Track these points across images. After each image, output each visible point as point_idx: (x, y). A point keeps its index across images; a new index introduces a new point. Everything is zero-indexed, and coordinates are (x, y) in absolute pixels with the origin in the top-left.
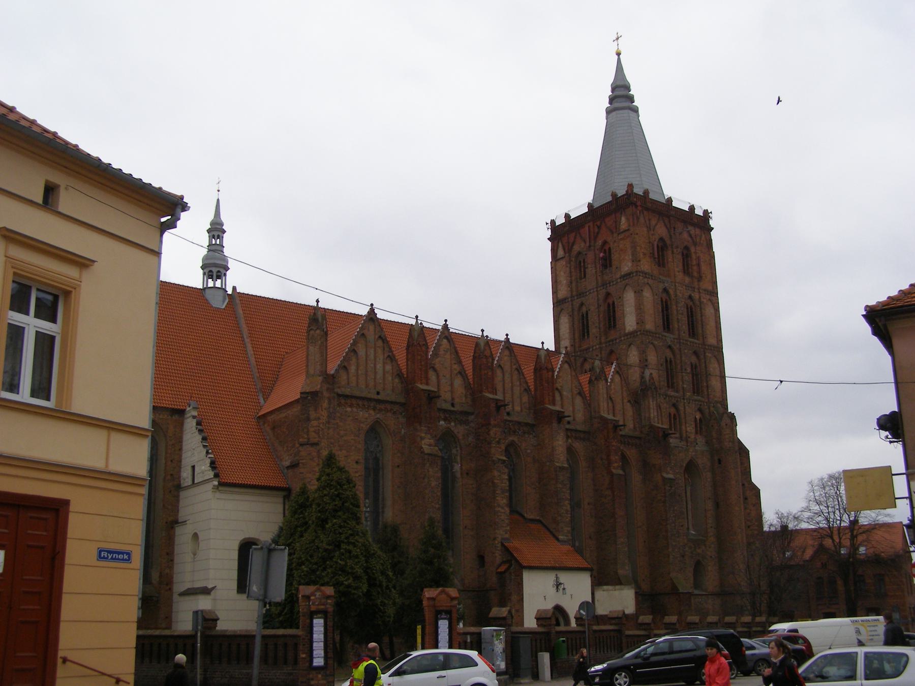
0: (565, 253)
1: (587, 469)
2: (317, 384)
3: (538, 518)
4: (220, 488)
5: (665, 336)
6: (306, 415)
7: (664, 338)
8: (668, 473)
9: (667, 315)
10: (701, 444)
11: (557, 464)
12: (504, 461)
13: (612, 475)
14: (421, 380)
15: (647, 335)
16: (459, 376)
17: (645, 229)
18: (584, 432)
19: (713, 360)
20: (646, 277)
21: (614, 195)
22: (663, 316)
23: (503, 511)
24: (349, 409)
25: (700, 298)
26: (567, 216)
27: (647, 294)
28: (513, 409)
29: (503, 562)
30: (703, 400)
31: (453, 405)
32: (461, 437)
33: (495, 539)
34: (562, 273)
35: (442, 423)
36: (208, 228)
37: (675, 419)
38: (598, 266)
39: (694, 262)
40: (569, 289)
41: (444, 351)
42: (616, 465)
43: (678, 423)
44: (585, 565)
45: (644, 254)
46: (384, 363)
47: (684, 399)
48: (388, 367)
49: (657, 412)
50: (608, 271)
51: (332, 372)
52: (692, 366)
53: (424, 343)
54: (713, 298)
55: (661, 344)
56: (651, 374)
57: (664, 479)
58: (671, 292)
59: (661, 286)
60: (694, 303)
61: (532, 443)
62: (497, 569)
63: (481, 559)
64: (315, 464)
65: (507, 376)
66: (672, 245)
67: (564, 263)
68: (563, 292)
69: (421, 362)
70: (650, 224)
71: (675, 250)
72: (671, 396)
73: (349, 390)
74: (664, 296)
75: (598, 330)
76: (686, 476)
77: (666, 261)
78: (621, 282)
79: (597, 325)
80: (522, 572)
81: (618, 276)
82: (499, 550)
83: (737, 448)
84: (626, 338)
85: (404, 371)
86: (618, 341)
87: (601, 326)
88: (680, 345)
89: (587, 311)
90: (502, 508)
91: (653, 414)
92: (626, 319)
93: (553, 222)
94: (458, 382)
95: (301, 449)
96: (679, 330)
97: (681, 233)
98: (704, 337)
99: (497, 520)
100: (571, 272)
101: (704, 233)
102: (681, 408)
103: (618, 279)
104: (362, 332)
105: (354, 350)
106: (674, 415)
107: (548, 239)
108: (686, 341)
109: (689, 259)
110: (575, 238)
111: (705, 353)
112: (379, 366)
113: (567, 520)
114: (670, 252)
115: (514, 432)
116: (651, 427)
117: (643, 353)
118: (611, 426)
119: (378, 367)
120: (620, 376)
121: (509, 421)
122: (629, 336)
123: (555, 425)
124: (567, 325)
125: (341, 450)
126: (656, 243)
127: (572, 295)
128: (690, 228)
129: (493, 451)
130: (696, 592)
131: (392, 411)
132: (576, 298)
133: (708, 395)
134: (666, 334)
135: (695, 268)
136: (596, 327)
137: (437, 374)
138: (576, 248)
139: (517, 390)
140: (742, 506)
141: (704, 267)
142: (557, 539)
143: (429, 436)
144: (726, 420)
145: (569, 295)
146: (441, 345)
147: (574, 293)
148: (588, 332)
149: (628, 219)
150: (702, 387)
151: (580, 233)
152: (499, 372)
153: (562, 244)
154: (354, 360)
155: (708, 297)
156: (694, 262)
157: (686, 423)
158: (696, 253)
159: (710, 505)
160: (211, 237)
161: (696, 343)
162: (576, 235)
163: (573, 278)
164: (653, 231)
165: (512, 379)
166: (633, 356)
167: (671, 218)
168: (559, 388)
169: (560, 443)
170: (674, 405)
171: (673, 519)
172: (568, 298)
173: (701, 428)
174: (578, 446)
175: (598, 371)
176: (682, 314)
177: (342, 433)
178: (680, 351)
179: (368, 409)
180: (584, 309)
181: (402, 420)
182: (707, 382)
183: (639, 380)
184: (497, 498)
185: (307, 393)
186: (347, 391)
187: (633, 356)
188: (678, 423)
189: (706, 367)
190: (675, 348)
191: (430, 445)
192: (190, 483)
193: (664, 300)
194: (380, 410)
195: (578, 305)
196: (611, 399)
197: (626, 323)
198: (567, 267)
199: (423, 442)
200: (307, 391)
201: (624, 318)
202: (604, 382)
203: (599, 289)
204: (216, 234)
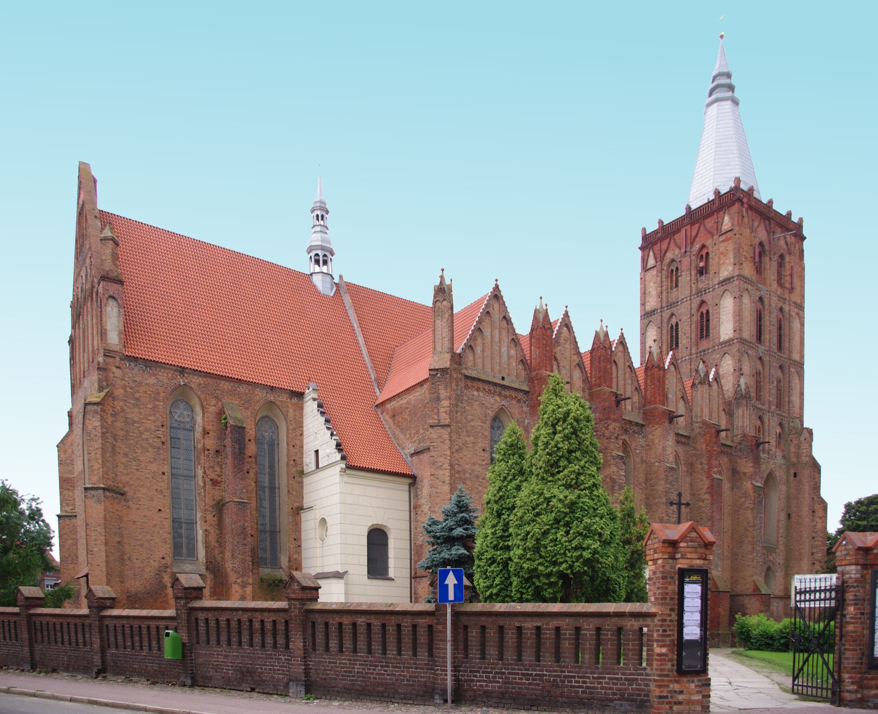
2: (445, 361)
9: (760, 326)
12: (622, 458)
18: (685, 437)
19: (796, 377)
24: (476, 393)
26: (661, 222)
38: (693, 273)
42: (716, 469)
46: (509, 347)
48: (513, 352)
50: (703, 277)
51: (458, 351)
55: (754, 354)
65: (620, 372)
92: (721, 327)
95: (431, 430)
98: (790, 352)
103: (714, 286)
106: (759, 427)
108: (775, 353)
110: (669, 244)
112: (504, 349)
125: (469, 436)
133: (789, 410)
134: (759, 346)
138: (669, 256)
144: (805, 434)
154: (480, 341)
157: (769, 436)
165: (625, 377)
174: (680, 449)
175: (702, 375)
177: (470, 417)
182: (789, 397)
185: (437, 370)
186: (474, 374)
194: (506, 397)
197: (721, 331)
200: (437, 368)
203: (692, 297)
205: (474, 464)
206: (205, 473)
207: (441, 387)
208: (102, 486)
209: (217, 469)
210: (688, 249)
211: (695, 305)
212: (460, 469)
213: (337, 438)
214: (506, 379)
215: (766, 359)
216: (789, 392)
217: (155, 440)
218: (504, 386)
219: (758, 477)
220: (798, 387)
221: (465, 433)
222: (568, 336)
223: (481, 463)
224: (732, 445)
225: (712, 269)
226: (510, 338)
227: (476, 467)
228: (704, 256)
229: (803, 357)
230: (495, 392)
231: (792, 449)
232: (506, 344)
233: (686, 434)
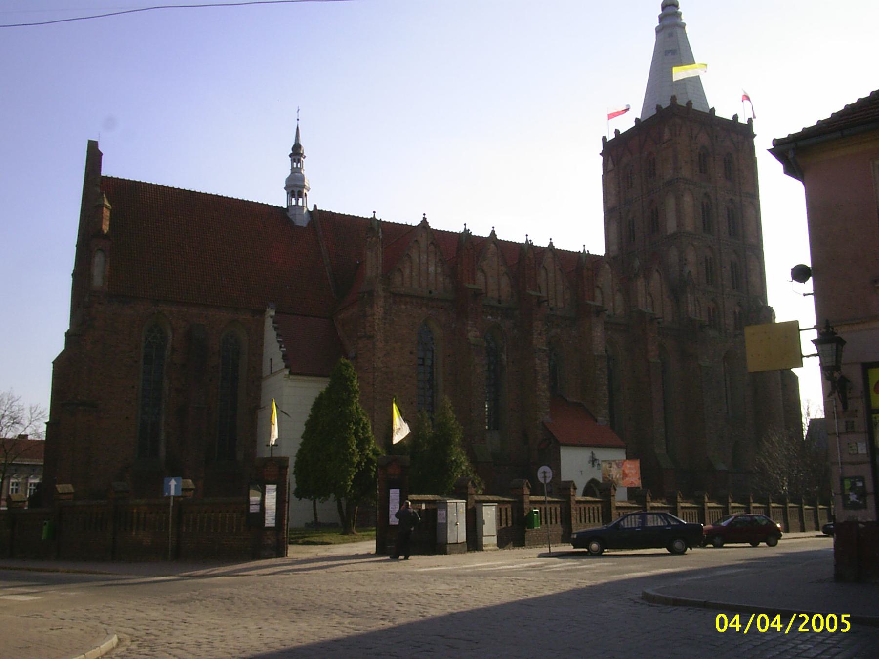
0: (614, 166)
4: (291, 377)
12: (545, 350)
21: (659, 108)
24: (403, 307)
26: (617, 132)
27: (687, 199)
28: (556, 305)
31: (499, 302)
35: (489, 317)
36: (289, 154)
41: (492, 254)
46: (436, 266)
53: (471, 247)
56: (690, 272)
65: (551, 275)
80: (560, 448)
93: (604, 138)
94: (505, 282)
104: (415, 239)
105: (408, 254)
107: (600, 154)
112: (432, 269)
119: (430, 269)
129: (534, 342)
142: (596, 421)
143: (475, 329)
152: (543, 272)
160: (293, 160)
168: (600, 285)
169: (598, 333)
170: (713, 300)
184: (539, 384)
192: (269, 374)
199: (469, 334)
204: (297, 157)
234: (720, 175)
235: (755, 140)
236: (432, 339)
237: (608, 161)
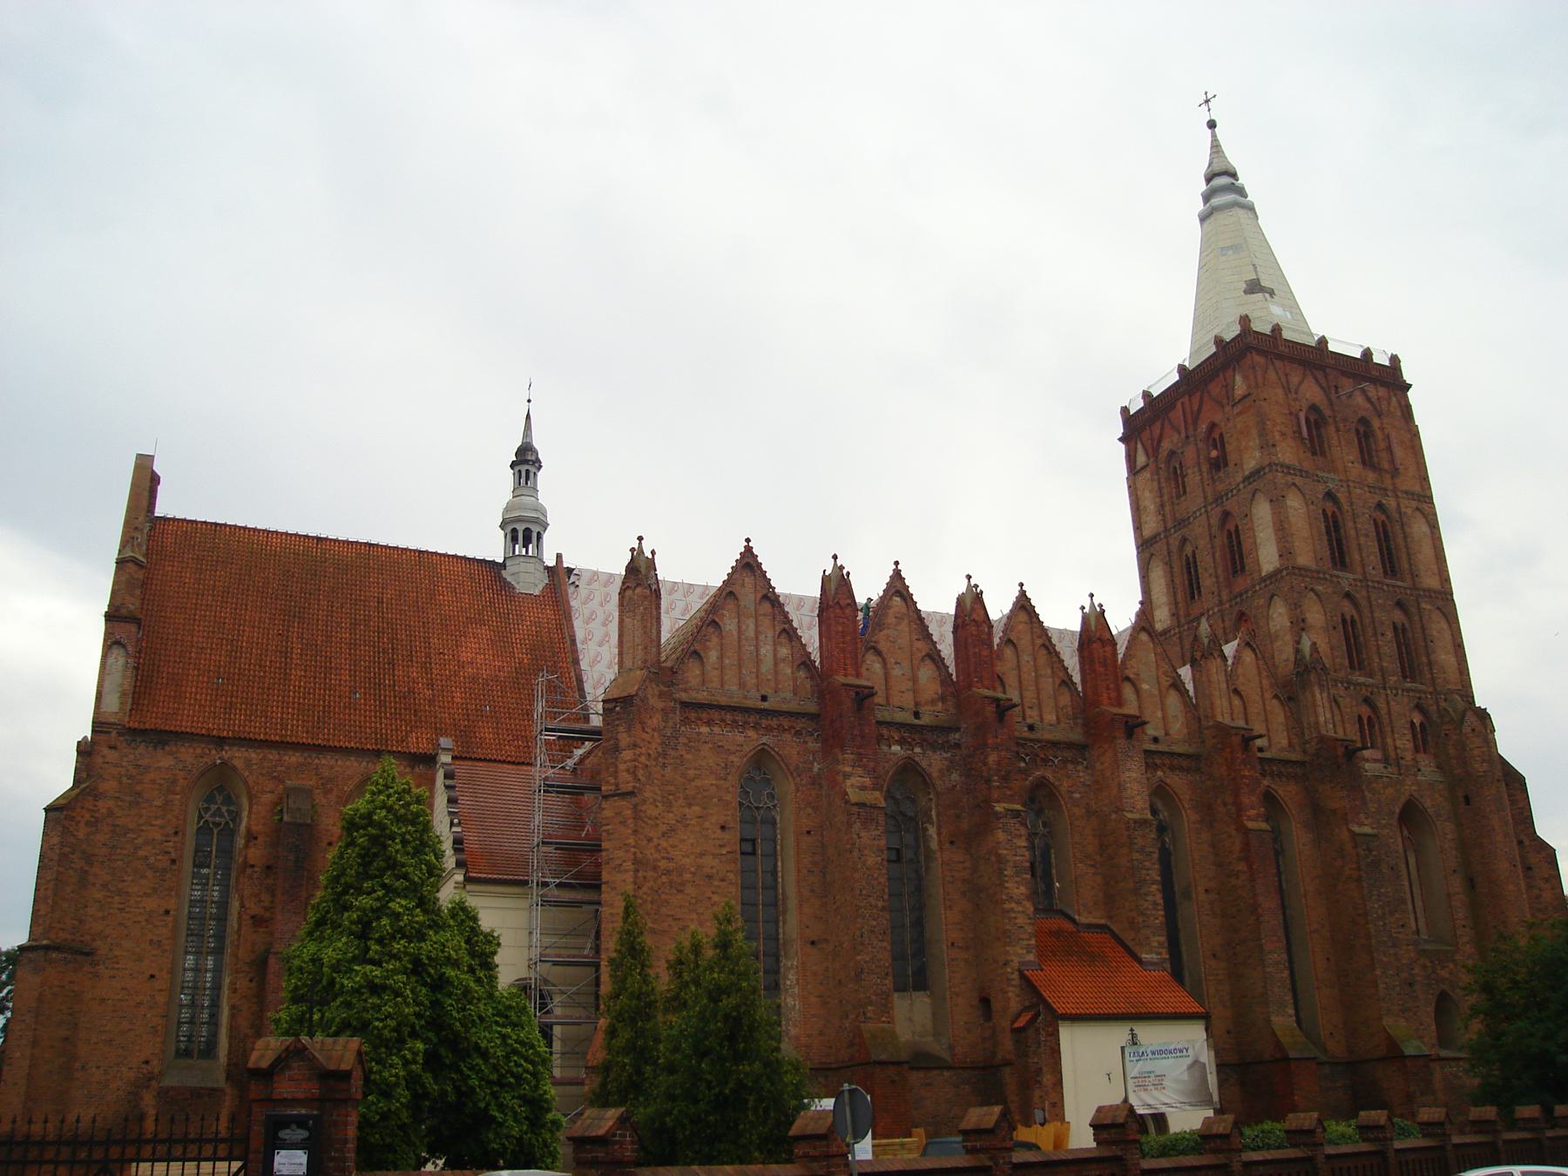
1: (1199, 826)
3: (1103, 921)
5: (1337, 577)
6: (612, 742)
7: (1334, 579)
8: (1361, 824)
10: (1428, 770)
11: (1129, 815)
13: (1246, 832)
14: (845, 669)
15: (1301, 575)
16: (928, 661)
17: (1280, 391)
19: (1436, 616)
20: (1290, 474)
21: (1219, 341)
22: (1330, 540)
23: (1020, 909)
24: (704, 729)
25: (1398, 505)
26: (1146, 395)
27: (1294, 503)
28: (1042, 720)
29: (1026, 1009)
30: (1423, 687)
31: (917, 715)
32: (935, 775)
33: (1006, 964)
34: (1147, 494)
35: (896, 748)
37: (1371, 726)
38: (1205, 468)
39: (1382, 445)
40: (1160, 517)
42: (1252, 812)
43: (1378, 733)
44: (1196, 1008)
45: (1283, 434)
47: (1385, 689)
49: (1332, 712)
50: (1221, 474)
51: (669, 664)
52: (1395, 628)
53: (849, 601)
54: (1425, 506)
55: (1330, 590)
56: (1314, 644)
57: (1354, 835)
58: (1342, 497)
59: (1321, 489)
60: (1388, 517)
61: (1082, 780)
62: (1014, 1022)
63: (985, 1002)
64: (630, 831)
65: (1025, 658)
66: (1335, 417)
67: (1148, 476)
68: (1152, 525)
69: (844, 637)
70: (1288, 382)
71: (1341, 425)
72: (1359, 684)
73: (705, 694)
74: (1330, 507)
75: (1214, 580)
76: (1406, 833)
77: (1326, 446)
78: (1244, 487)
79: (1212, 571)
81: (1240, 479)
82: (1014, 986)
83: (1499, 774)
84: (1263, 585)
85: (816, 657)
86: (1250, 594)
87: (1220, 571)
88: (1368, 591)
89: (1194, 552)
90: (1019, 903)
91: (1324, 715)
94: (926, 673)
96: (1363, 565)
97: (1350, 396)
99: (1008, 927)
100: (1160, 489)
101: (1395, 395)
102: (1381, 704)
103: (1238, 485)
104: (729, 589)
105: (714, 621)
107: (1120, 439)
108: (1378, 582)
109: (1371, 440)
110: (1162, 428)
111: (1419, 604)
112: (766, 650)
113: (1157, 921)
114: (1332, 429)
115: (1045, 761)
116: (1322, 739)
117: (1295, 607)
118: (1236, 740)
119: (763, 651)
120: (1254, 650)
121: (1031, 740)
122: (1268, 582)
123: (1121, 742)
124: (1162, 581)
125: (690, 805)
126: (1302, 416)
127: (1165, 527)
128: (1372, 391)
130: (1444, 1053)
131: (793, 731)
132: (1173, 531)
133: (1433, 679)
134: (1340, 574)
135: (1384, 455)
136: (1211, 575)
137: (884, 660)
138: (1166, 445)
139: (1048, 684)
140: (1523, 884)
141: (1399, 453)
142: (1140, 961)
143: (860, 771)
144: (1471, 719)
145: (1162, 529)
146: (889, 608)
147: (1170, 525)
148: (1199, 588)
149: (1245, 377)
150: (1419, 665)
151: (1170, 421)
153: (1143, 444)
155: (1414, 504)
156: (1382, 445)
157: (1393, 732)
158: (1382, 429)
159: (1457, 884)
161: (1399, 587)
162: (1163, 425)
163: (1166, 498)
164: (1296, 393)
166: (1279, 616)
167: (1328, 370)
168: (1132, 676)
170: (1366, 701)
171: (1380, 912)
172: (1160, 534)
173: (1425, 742)
174: (1177, 781)
175: (1206, 641)
176: (1366, 536)
178: (1370, 602)
179: (744, 728)
180: (1188, 549)
181: (813, 745)
182: (1428, 655)
183: (1292, 658)
184: (1006, 885)
185: (615, 700)
186: (702, 696)
187: (1279, 616)
188: (1378, 733)
189: (1423, 629)
190: (1357, 596)
191: (863, 788)
193: (1329, 514)
194: (769, 729)
195: (1177, 543)
196: (1236, 692)
197: (1260, 560)
198: (1152, 480)
199: (848, 783)
200: (615, 696)
201: (1257, 551)
202: (1219, 660)
203: (1209, 508)
204: (524, 468)
205: (702, 855)
206: (242, 905)
207: (621, 729)
208: (45, 942)
209: (265, 897)
210: (1191, 433)
211: (1215, 521)
212: (671, 865)
213: (459, 829)
214: (771, 699)
215: (1360, 595)
216: (1426, 646)
217: (159, 857)
218: (765, 710)
219: (1362, 816)
220: (1447, 636)
221: (681, 801)
222: (904, 610)
223: (717, 851)
224: (1307, 759)
225: (1232, 458)
226: (778, 629)
227: (708, 861)
228: (1215, 438)
229: (1448, 580)
230: (746, 723)
231: (1452, 751)
232: (770, 640)
233: (1191, 750)
234: (1352, 458)
235: (1410, 393)
236: (771, 796)
237: (1136, 450)
